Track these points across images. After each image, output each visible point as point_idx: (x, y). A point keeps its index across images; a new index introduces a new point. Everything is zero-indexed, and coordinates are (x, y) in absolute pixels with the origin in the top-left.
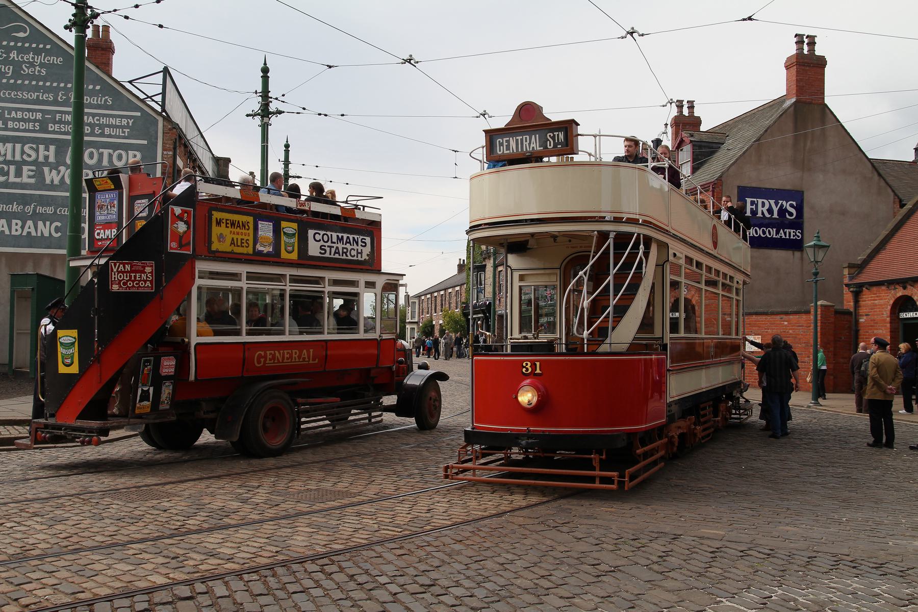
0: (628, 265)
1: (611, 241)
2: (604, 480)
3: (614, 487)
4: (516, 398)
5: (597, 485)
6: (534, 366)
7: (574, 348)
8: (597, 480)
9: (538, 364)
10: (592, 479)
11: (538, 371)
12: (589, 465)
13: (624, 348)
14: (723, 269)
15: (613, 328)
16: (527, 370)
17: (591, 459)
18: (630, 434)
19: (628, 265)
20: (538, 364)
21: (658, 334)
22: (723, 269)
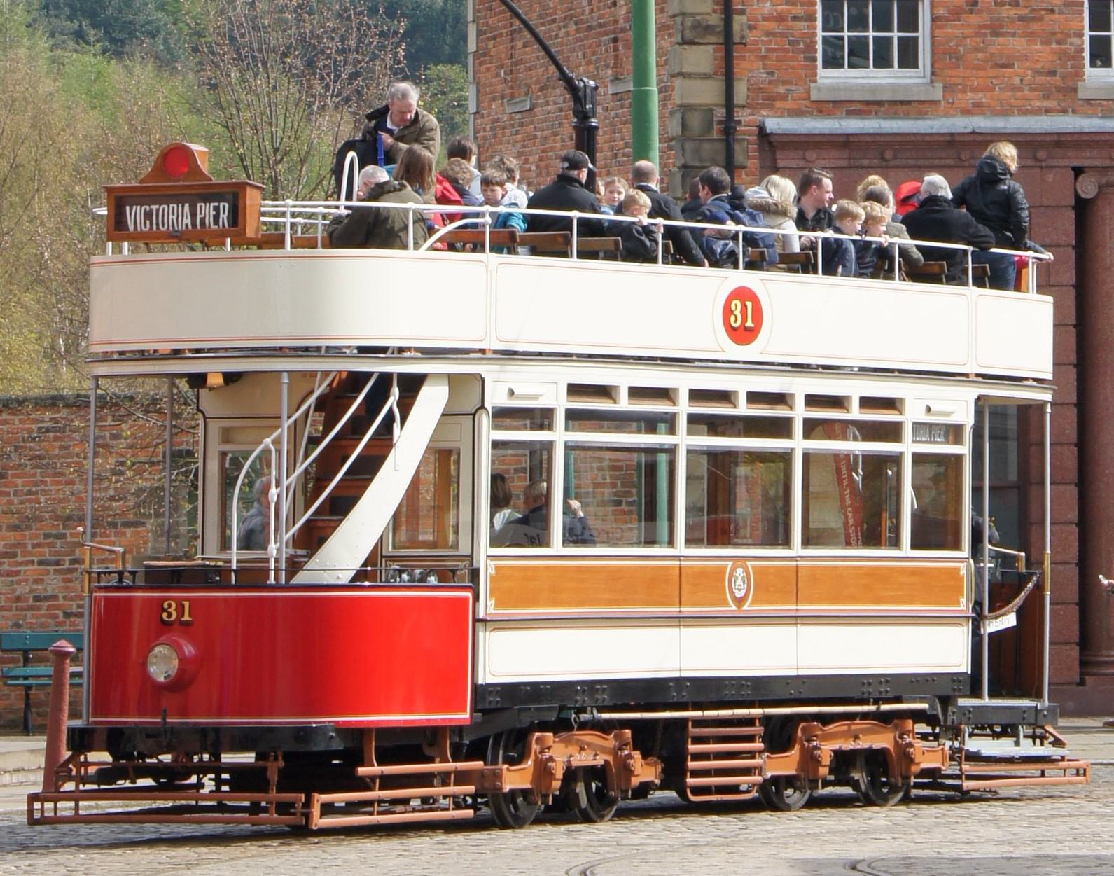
0: (357, 426)
4: (144, 665)
6: (180, 609)
7: (253, 576)
9: (187, 604)
11: (186, 618)
13: (345, 578)
16: (170, 615)
18: (357, 735)
20: (187, 604)
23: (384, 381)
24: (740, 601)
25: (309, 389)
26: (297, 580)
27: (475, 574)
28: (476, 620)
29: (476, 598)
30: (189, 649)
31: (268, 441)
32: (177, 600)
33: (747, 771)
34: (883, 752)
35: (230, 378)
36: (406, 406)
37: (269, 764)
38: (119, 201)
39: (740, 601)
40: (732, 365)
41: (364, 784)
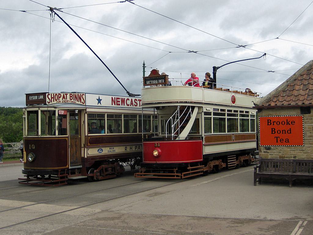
0: (185, 114)
1: (178, 109)
2: (177, 176)
3: (180, 178)
5: (175, 177)
7: (169, 138)
8: (175, 176)
10: (174, 176)
11: (159, 146)
12: (172, 172)
14: (239, 110)
15: (180, 133)
17: (173, 170)
18: (187, 164)
19: (185, 114)
21: (200, 134)
22: (239, 110)
23: (189, 107)
24: (233, 140)
25: (176, 108)
26: (177, 139)
27: (202, 138)
28: (203, 145)
29: (203, 141)
30: (160, 151)
31: (171, 117)
32: (157, 143)
33: (234, 164)
34: (248, 160)
35: (163, 107)
36: (192, 111)
37: (174, 169)
38: (146, 80)
39: (233, 140)
40: (232, 106)
41: (188, 170)
